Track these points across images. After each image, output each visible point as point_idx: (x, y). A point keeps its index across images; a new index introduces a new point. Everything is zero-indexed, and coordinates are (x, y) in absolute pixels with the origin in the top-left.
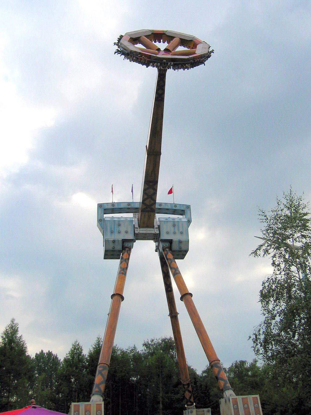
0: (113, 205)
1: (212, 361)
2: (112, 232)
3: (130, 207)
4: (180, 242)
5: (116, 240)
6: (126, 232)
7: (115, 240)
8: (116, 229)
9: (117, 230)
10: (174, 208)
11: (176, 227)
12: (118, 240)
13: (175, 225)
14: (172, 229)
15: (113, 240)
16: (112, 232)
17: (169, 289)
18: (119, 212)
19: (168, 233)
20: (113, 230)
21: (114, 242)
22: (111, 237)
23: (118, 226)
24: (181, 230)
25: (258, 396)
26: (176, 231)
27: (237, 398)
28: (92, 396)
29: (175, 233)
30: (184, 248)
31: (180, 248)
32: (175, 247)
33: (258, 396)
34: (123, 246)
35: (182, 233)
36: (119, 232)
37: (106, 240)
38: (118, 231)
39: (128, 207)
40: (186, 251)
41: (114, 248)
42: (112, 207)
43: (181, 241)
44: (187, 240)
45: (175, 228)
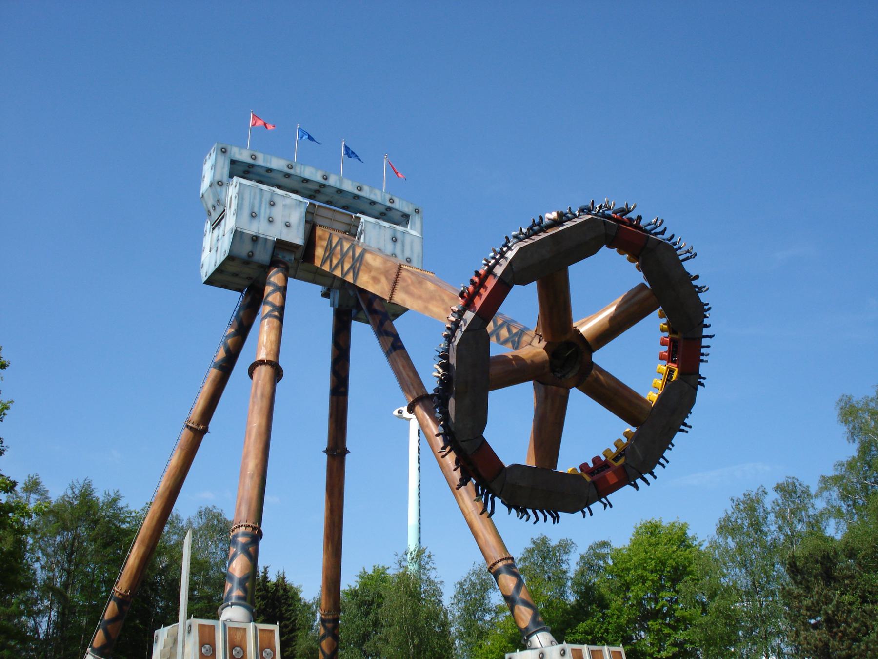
1: (494, 561)
2: (253, 216)
3: (291, 172)
5: (262, 236)
6: (286, 225)
7: (258, 235)
8: (263, 211)
10: (389, 204)
11: (399, 245)
12: (266, 239)
13: (396, 240)
15: (254, 234)
16: (253, 216)
17: (342, 389)
18: (258, 178)
20: (256, 210)
21: (255, 239)
22: (252, 228)
23: (268, 205)
24: (408, 254)
25: (276, 628)
27: (581, 650)
28: (223, 609)
33: (276, 628)
34: (273, 255)
36: (271, 221)
37: (239, 230)
38: (267, 217)
41: (251, 255)
42: (250, 161)
45: (395, 245)
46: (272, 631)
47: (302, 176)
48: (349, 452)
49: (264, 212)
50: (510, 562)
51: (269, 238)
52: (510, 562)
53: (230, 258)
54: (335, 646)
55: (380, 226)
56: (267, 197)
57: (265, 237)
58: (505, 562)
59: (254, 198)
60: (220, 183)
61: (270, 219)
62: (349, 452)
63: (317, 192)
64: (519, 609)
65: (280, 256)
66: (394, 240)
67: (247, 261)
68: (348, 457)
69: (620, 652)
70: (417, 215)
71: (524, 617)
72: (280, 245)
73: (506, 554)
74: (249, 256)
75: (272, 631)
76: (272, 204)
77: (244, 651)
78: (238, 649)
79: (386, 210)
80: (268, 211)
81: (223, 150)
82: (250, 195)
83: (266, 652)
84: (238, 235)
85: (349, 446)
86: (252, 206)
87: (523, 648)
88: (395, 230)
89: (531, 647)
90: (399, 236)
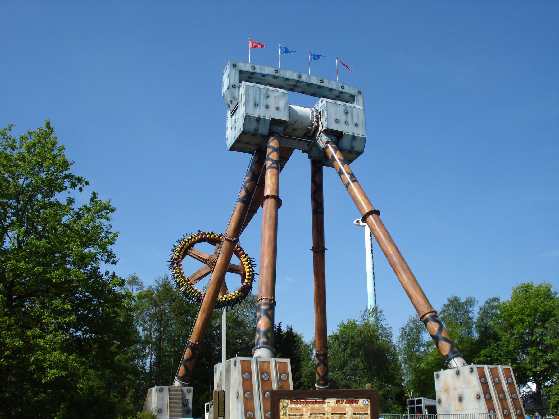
0: (253, 67)
1: (424, 314)
2: (256, 105)
3: (278, 75)
4: (354, 138)
5: (262, 117)
6: (277, 109)
8: (262, 102)
9: (263, 103)
10: (341, 90)
11: (349, 115)
12: (265, 119)
13: (347, 112)
14: (343, 118)
15: (257, 116)
16: (256, 105)
17: (320, 210)
19: (337, 121)
20: (257, 101)
21: (258, 120)
22: (256, 113)
23: (265, 97)
24: (355, 121)
25: (288, 361)
26: (349, 120)
27: (483, 368)
28: (255, 350)
29: (347, 123)
30: (357, 148)
31: (352, 147)
32: (346, 143)
33: (288, 361)
34: (270, 129)
35: (356, 125)
36: (267, 107)
37: (248, 115)
38: (265, 105)
39: (274, 74)
40: (359, 153)
41: (256, 130)
42: (251, 70)
43: (355, 137)
44: (363, 136)
45: (347, 116)
46: (286, 363)
47: (285, 76)
48: (326, 249)
49: (263, 102)
50: (434, 314)
51: (266, 118)
52: (434, 314)
53: (244, 133)
54: (326, 370)
55: (337, 104)
56: (263, 92)
57: (264, 118)
58: (430, 314)
59: (256, 94)
60: (234, 86)
61: (267, 106)
62: (326, 249)
63: (295, 86)
64: (441, 343)
65: (275, 129)
66: (346, 112)
67: (255, 134)
68: (326, 252)
69: (509, 369)
70: (359, 95)
71: (445, 349)
72: (275, 122)
73: (431, 309)
74: (255, 131)
75: (286, 363)
76: (267, 97)
77: (269, 376)
78: (266, 374)
79: (340, 93)
80: (265, 101)
81: (234, 65)
82: (253, 92)
83: (283, 376)
84: (247, 118)
85: (326, 245)
86: (255, 99)
87: (446, 368)
88: (346, 106)
89: (451, 367)
90: (349, 110)
